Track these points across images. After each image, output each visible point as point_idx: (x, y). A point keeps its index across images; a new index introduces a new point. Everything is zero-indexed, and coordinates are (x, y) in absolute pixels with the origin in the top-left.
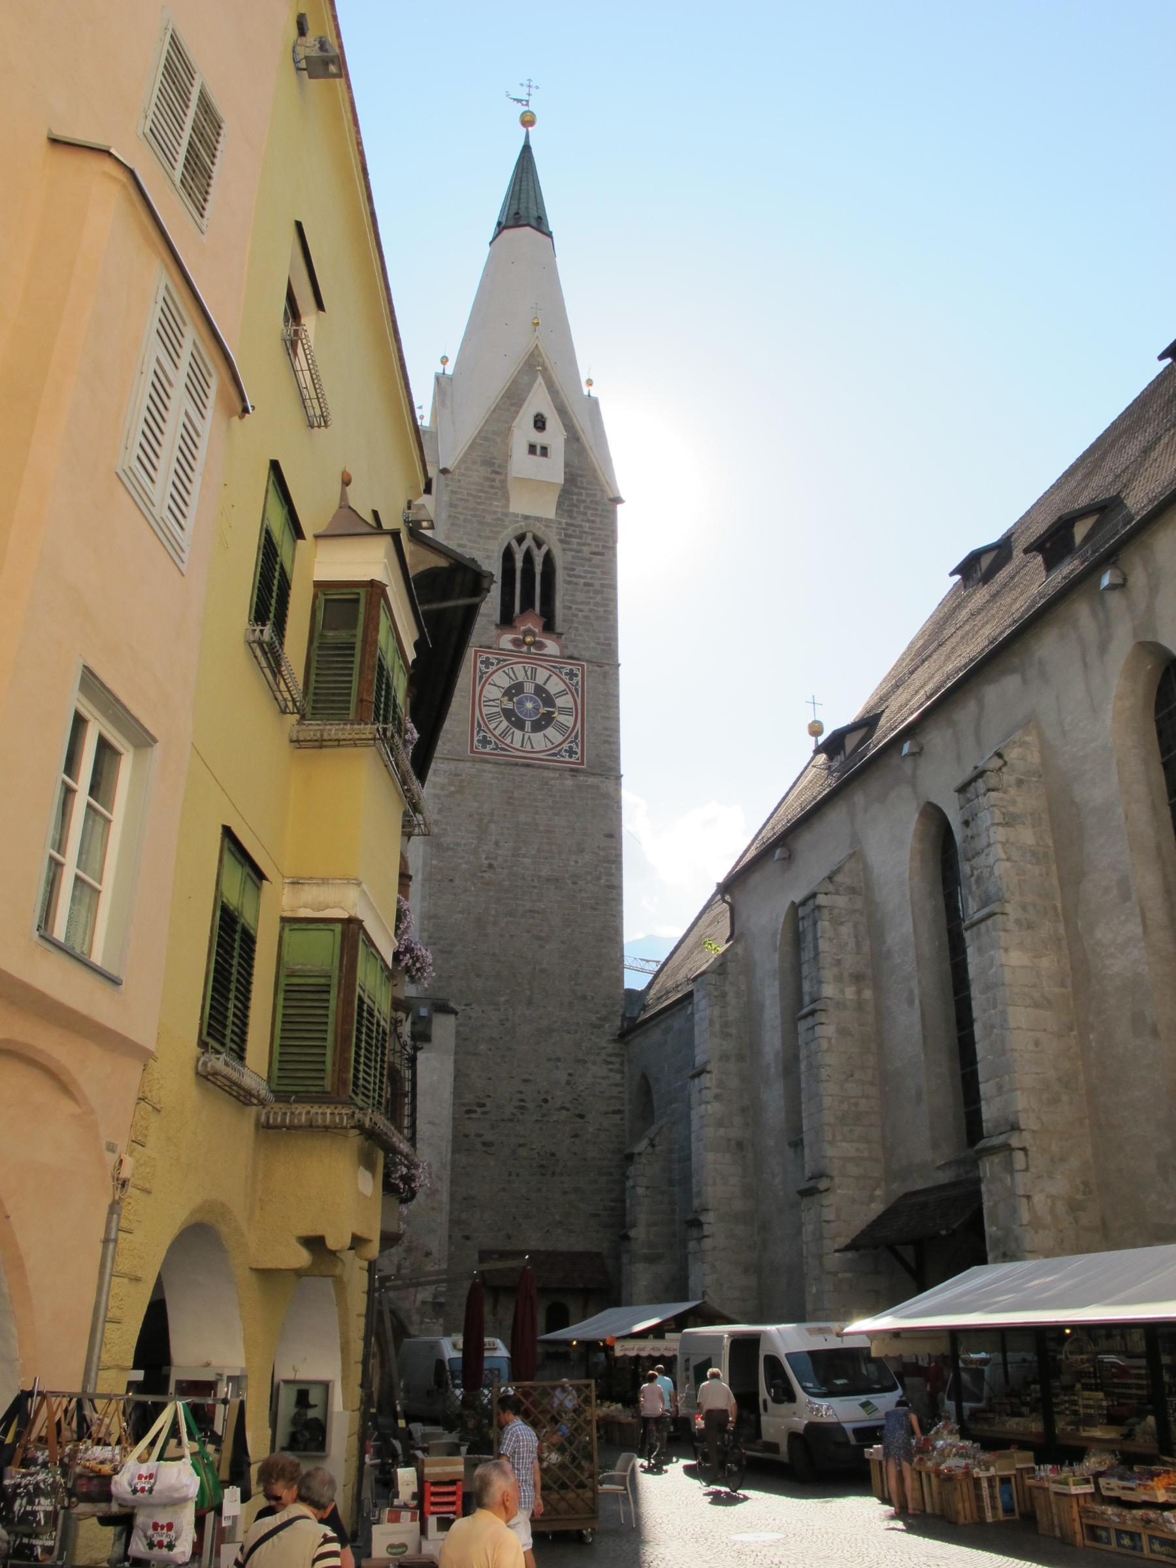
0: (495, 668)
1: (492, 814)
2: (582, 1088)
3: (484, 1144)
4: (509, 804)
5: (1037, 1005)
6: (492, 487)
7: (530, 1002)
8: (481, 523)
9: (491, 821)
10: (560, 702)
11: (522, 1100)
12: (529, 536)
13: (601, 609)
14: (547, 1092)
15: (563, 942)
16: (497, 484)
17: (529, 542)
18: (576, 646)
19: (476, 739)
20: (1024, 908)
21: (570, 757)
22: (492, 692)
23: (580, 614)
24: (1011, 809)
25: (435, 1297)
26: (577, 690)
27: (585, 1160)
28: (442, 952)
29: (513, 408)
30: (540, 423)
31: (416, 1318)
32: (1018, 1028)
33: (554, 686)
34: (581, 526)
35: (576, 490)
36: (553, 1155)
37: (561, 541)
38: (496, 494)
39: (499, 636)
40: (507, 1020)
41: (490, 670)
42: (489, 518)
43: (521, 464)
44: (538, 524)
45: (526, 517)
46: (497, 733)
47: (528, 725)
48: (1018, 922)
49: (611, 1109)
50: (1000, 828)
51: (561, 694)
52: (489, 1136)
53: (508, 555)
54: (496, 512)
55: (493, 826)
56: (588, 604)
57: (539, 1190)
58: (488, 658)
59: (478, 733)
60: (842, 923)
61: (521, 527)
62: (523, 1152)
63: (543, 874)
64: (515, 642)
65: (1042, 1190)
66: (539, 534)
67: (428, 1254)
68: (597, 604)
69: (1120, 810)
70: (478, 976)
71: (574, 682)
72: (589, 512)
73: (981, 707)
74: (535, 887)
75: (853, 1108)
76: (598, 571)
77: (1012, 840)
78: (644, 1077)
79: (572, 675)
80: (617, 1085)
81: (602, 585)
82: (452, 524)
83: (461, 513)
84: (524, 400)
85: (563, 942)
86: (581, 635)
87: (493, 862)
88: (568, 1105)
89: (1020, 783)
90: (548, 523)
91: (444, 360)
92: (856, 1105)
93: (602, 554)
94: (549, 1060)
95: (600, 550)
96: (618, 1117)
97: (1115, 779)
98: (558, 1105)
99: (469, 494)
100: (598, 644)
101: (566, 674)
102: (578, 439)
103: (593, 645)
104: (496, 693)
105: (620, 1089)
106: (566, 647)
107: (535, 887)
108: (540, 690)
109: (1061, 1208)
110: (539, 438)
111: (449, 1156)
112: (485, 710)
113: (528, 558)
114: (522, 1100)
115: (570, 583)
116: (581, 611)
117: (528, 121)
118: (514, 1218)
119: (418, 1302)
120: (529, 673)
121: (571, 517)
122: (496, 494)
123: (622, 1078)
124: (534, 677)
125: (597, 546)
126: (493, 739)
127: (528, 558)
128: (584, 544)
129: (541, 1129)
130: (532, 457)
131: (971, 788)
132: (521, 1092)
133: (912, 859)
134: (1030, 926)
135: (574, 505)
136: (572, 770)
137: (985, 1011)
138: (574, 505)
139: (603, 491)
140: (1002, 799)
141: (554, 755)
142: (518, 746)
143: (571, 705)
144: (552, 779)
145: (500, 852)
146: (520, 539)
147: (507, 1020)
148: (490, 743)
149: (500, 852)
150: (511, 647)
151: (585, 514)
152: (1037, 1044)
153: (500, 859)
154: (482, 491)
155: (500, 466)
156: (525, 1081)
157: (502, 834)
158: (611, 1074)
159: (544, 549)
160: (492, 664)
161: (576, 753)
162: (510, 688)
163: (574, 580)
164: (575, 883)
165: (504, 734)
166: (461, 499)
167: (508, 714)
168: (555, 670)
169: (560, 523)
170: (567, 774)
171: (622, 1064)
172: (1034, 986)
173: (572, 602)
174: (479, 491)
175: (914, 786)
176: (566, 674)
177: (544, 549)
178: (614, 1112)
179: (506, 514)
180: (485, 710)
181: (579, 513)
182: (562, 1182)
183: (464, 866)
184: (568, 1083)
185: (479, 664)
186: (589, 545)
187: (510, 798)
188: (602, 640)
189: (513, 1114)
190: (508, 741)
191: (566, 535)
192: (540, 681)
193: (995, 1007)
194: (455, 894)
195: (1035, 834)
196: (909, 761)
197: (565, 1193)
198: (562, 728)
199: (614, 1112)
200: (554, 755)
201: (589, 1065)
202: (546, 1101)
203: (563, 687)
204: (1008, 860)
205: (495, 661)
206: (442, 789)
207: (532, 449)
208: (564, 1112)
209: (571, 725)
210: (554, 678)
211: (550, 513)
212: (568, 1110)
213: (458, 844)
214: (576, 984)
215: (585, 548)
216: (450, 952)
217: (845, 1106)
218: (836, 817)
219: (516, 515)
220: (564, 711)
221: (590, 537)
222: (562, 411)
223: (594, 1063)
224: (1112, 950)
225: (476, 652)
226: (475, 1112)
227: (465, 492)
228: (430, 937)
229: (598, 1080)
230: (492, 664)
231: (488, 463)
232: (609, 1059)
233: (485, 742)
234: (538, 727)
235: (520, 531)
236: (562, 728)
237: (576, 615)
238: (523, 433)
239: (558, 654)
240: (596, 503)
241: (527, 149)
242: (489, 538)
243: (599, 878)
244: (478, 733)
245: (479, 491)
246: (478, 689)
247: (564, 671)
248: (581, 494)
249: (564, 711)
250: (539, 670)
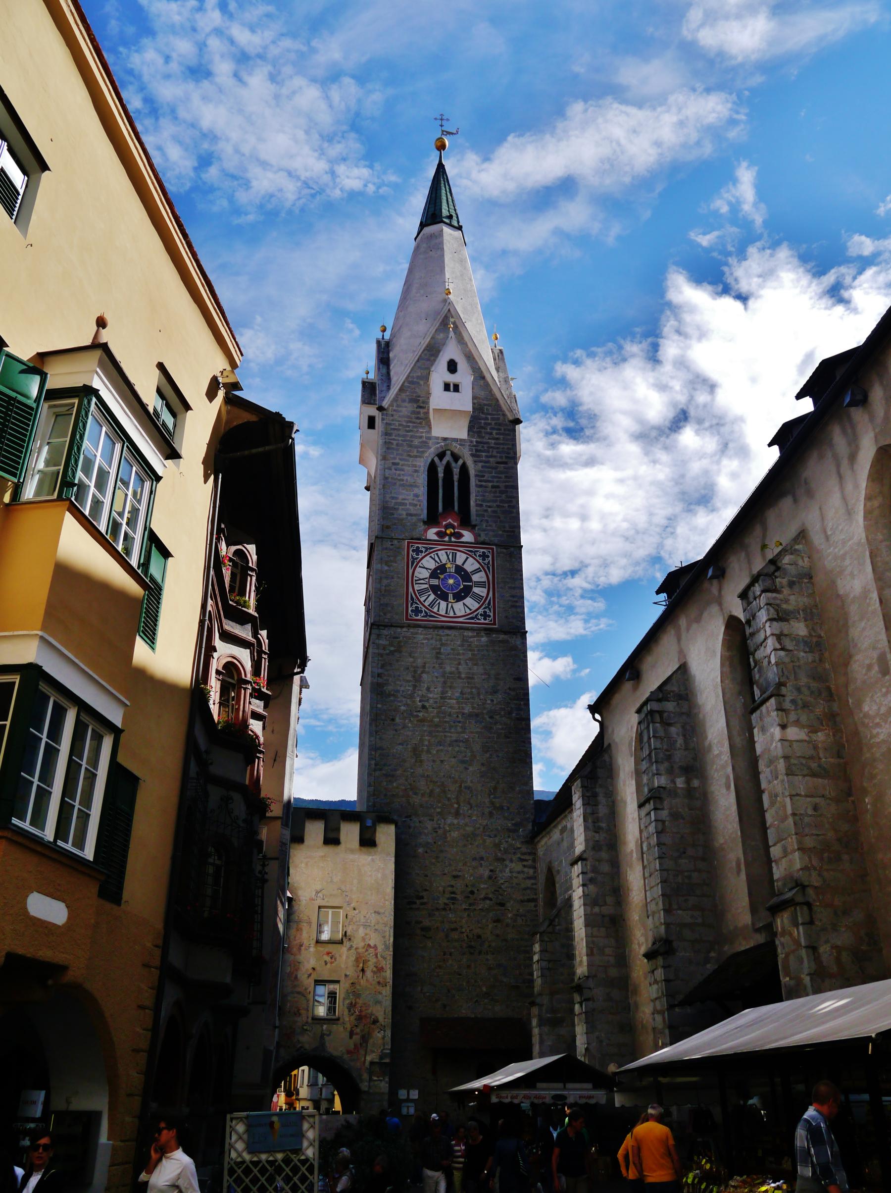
0: (423, 554)
1: (424, 667)
2: (502, 881)
3: (423, 929)
4: (437, 658)
5: (814, 775)
6: (418, 418)
7: (457, 814)
8: (410, 446)
9: (422, 673)
10: (476, 578)
11: (453, 893)
12: (448, 453)
13: (506, 505)
14: (473, 886)
15: (483, 764)
16: (422, 415)
17: (448, 458)
18: (486, 535)
19: (410, 609)
20: (798, 690)
21: (485, 619)
22: (422, 574)
23: (489, 509)
24: (784, 606)
25: (381, 1058)
26: (488, 568)
27: (506, 940)
28: (386, 775)
29: (432, 358)
30: (452, 367)
31: (365, 1076)
32: (797, 795)
33: (471, 565)
34: (488, 443)
35: (484, 416)
36: (479, 937)
37: (472, 455)
38: (421, 423)
39: (426, 531)
40: (440, 828)
41: (420, 557)
42: (416, 442)
43: (438, 399)
44: (454, 444)
45: (445, 439)
46: (426, 604)
47: (451, 596)
48: (793, 702)
49: (526, 898)
50: (775, 623)
51: (477, 571)
52: (426, 923)
53: (432, 469)
54: (421, 437)
55: (425, 676)
56: (496, 501)
57: (469, 967)
58: (418, 548)
59: (412, 605)
60: (670, 725)
61: (441, 446)
62: (455, 935)
63: (466, 711)
64: (438, 534)
65: (827, 942)
66: (456, 451)
67: (375, 1021)
68: (502, 501)
69: (875, 596)
70: (416, 794)
71: (486, 561)
72: (494, 432)
73: (765, 530)
74: (459, 722)
75: (687, 881)
76: (503, 476)
77: (786, 632)
78: (550, 870)
79: (484, 556)
80: (529, 878)
81: (507, 487)
82: (388, 448)
83: (394, 439)
84: (439, 351)
85: (483, 764)
86: (490, 526)
87: (427, 704)
88: (491, 896)
89: (791, 584)
90: (461, 442)
92: (689, 877)
93: (505, 463)
94: (474, 859)
95: (504, 460)
96: (532, 904)
97: (869, 569)
98: (482, 896)
99: (400, 425)
100: (504, 531)
101: (480, 556)
102: (483, 378)
103: (500, 532)
104: (426, 574)
105: (533, 881)
106: (480, 535)
107: (459, 722)
108: (459, 569)
109: (845, 957)
110: (452, 379)
111: (392, 940)
112: (417, 587)
114: (453, 893)
115: (481, 486)
116: (490, 507)
118: (449, 991)
119: (367, 1064)
120: (450, 557)
121: (479, 437)
122: (421, 423)
123: (535, 872)
125: (501, 457)
126: (423, 608)
127: (448, 469)
128: (491, 456)
129: (468, 915)
130: (446, 393)
131: (751, 594)
132: (452, 886)
133: (722, 665)
134: (805, 706)
135: (482, 428)
136: (486, 629)
137: (770, 782)
138: (482, 428)
139: (504, 415)
140: (775, 598)
141: (472, 618)
142: (443, 612)
143: (484, 579)
144: (471, 637)
145: (431, 695)
146: (441, 456)
147: (440, 828)
148: (421, 611)
149: (431, 695)
150: (436, 538)
151: (491, 434)
152: (815, 808)
153: (431, 701)
154: (411, 422)
155: (423, 402)
156: (455, 877)
157: (433, 681)
158: (526, 870)
159: (460, 462)
160: (422, 552)
161: (489, 616)
162: (436, 569)
163: (484, 484)
164: (491, 717)
165: (432, 604)
166: (394, 429)
167: (434, 589)
168: (471, 554)
169: (472, 442)
170: (483, 633)
171: (534, 860)
172: (812, 758)
173: (483, 501)
174: (408, 422)
175: (720, 604)
176: (480, 556)
177: (460, 462)
178: (529, 901)
179: (430, 438)
180: (417, 587)
181: (487, 433)
182: (487, 960)
183: (403, 708)
184: (490, 877)
185: (411, 552)
186: (495, 457)
187: (438, 653)
188: (507, 529)
189: (446, 904)
190: (435, 610)
191: (477, 451)
192: (459, 562)
193: (777, 778)
194: (396, 730)
195: (807, 626)
196: (715, 582)
197: (490, 969)
199: (529, 901)
200: (472, 618)
201: (507, 862)
202: (472, 892)
203: (477, 566)
204: (782, 649)
205: (423, 550)
206: (384, 649)
207: (447, 387)
208: (488, 902)
209: (484, 595)
210: (471, 560)
211: (463, 434)
212: (491, 899)
213: (398, 691)
214: (495, 798)
215: (491, 459)
216: (393, 776)
217: (680, 879)
218: (668, 641)
219: (437, 438)
220: (480, 584)
221: (495, 451)
222: (471, 358)
223: (511, 861)
224: (878, 720)
225: (408, 543)
226: (415, 903)
227: (397, 423)
228: (376, 765)
229: (514, 875)
230: (422, 552)
231: (414, 400)
232: (523, 857)
233: (417, 611)
234: (459, 597)
235: (441, 450)
236: (477, 598)
237: (486, 511)
238: (439, 375)
239: (473, 540)
240: (500, 425)
241: (441, 168)
242: (416, 457)
243: (510, 713)
244: (412, 605)
245: (408, 422)
246: (411, 571)
247: (478, 554)
248: (487, 419)
249: (480, 584)
250: (458, 554)
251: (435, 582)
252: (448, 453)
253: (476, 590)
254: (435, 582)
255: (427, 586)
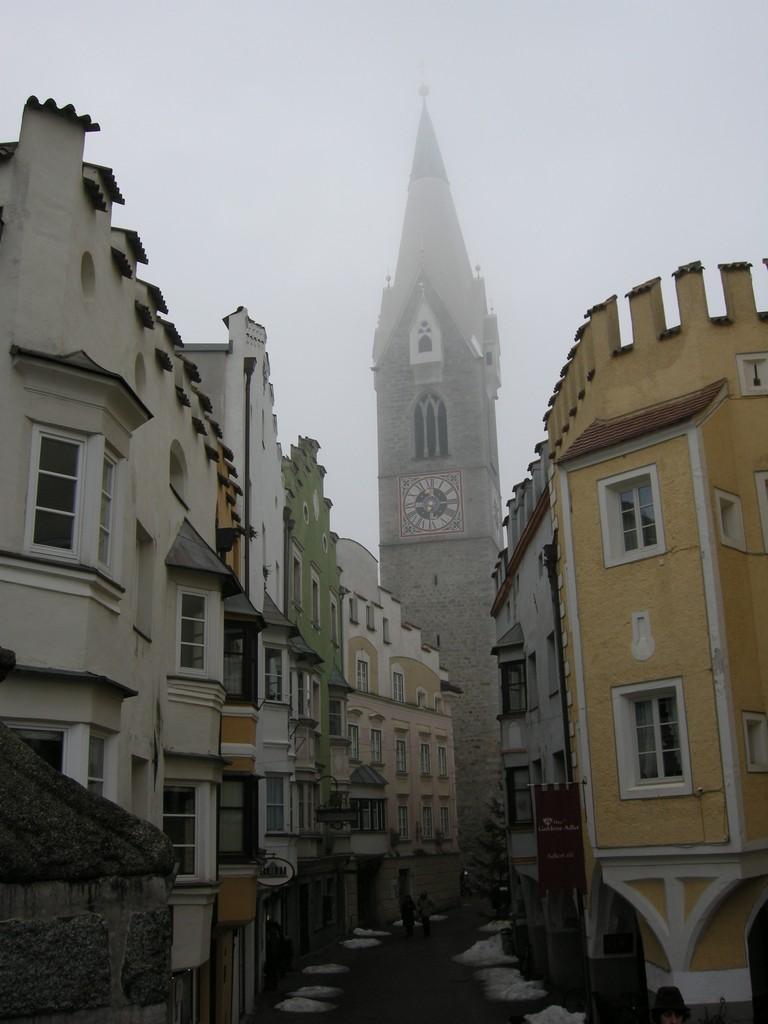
10: (449, 497)
12: (429, 396)
22: (410, 500)
47: (432, 515)
51: (449, 492)
53: (418, 410)
91: (389, 279)
104: (413, 500)
108: (437, 492)
112: (408, 511)
113: (430, 408)
117: (424, 92)
124: (432, 485)
127: (430, 408)
146: (423, 399)
167: (420, 511)
177: (438, 402)
192: (436, 487)
198: (452, 513)
203: (449, 487)
234: (438, 514)
236: (452, 513)
249: (453, 501)
250: (436, 480)
251: (419, 505)
252: (429, 396)
253: (449, 506)
254: (419, 505)
255: (413, 509)
